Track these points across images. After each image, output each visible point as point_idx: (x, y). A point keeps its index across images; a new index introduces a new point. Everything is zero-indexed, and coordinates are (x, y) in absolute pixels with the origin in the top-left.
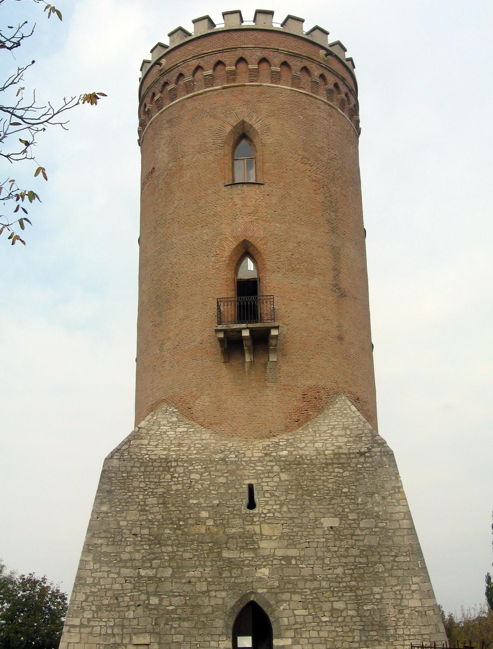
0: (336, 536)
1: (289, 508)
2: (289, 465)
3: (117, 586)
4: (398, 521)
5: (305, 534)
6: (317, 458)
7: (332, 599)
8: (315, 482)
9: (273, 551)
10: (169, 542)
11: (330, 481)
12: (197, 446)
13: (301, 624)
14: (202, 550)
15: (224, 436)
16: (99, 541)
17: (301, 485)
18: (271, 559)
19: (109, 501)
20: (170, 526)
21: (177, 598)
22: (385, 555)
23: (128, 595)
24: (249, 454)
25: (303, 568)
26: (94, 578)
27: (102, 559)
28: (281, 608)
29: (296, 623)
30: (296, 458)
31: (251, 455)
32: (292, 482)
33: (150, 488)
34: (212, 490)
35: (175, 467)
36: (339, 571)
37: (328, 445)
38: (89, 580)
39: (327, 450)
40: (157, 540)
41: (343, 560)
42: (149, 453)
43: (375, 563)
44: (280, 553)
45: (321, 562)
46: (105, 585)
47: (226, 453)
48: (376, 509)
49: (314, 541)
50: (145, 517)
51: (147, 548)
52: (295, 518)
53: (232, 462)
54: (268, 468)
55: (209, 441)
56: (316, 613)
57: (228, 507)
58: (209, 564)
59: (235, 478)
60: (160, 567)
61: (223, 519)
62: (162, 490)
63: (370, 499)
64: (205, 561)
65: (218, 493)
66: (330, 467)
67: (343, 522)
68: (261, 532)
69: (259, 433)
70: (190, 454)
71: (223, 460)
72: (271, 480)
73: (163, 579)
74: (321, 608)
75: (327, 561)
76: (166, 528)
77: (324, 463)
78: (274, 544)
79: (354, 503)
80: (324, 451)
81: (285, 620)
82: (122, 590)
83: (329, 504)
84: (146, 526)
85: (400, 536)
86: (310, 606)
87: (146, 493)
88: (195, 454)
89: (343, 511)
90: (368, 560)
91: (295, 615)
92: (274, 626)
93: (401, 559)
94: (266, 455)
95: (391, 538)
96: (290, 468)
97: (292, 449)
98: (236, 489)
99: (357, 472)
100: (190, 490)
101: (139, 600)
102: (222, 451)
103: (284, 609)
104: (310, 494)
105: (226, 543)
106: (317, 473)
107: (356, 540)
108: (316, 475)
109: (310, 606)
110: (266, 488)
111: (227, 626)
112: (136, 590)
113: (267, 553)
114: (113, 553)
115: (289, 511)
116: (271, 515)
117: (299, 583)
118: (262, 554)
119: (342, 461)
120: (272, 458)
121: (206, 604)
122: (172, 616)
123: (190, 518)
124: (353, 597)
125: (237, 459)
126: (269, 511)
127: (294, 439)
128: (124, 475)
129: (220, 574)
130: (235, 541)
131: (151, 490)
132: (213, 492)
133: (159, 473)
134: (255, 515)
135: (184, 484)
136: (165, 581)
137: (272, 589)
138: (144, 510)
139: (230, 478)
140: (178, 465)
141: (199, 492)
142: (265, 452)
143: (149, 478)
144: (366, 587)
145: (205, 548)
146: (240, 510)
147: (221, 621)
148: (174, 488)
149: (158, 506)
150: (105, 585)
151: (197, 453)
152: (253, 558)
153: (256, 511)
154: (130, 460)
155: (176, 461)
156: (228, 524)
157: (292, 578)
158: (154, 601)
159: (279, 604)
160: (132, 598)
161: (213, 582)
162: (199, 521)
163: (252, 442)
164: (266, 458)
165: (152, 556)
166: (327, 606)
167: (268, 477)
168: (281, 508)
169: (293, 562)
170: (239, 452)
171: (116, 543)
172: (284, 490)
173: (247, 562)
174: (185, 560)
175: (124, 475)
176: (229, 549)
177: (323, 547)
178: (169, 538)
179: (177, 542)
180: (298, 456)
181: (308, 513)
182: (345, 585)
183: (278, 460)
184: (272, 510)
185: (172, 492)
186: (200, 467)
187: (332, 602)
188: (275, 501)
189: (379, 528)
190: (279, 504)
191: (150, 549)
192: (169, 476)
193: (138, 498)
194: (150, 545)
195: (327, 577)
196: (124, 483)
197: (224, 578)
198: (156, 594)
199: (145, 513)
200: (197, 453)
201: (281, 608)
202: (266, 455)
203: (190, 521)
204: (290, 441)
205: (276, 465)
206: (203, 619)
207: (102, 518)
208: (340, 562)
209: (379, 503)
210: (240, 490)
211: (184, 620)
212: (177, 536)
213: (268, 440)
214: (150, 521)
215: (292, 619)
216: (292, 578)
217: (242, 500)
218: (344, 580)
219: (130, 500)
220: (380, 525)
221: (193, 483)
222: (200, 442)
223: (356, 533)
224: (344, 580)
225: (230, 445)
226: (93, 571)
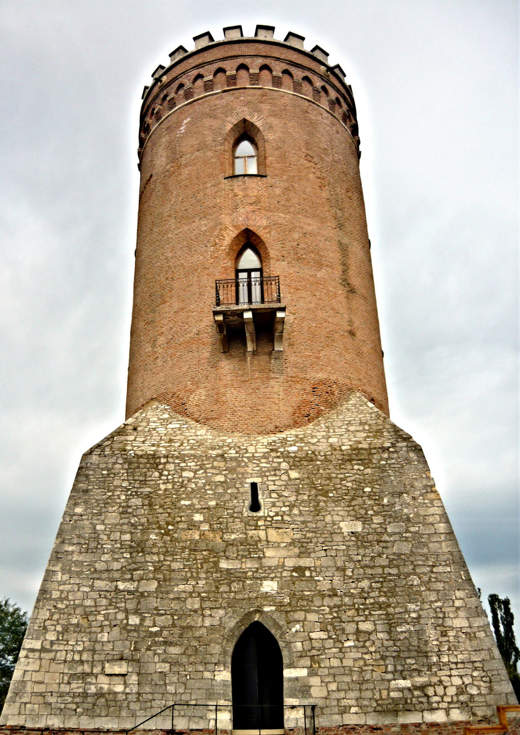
0: (359, 543)
1: (300, 511)
2: (300, 461)
3: (89, 603)
4: (433, 524)
5: (321, 540)
6: (332, 454)
7: (356, 619)
8: (331, 481)
9: (282, 560)
10: (155, 550)
11: (349, 479)
12: (191, 442)
13: (319, 650)
14: (195, 559)
15: (222, 432)
16: (71, 548)
17: (315, 485)
18: (280, 570)
19: (84, 502)
20: (157, 531)
21: (163, 618)
22: (419, 565)
23: (102, 612)
24: (251, 449)
25: (319, 581)
26: (62, 592)
27: (73, 569)
28: (294, 630)
29: (313, 648)
30: (308, 454)
31: (254, 451)
32: (303, 480)
33: (134, 487)
34: (208, 490)
35: (165, 464)
36: (365, 584)
37: (344, 441)
38: (56, 595)
39: (343, 445)
40: (139, 547)
41: (369, 571)
42: (135, 448)
43: (409, 575)
44: (290, 563)
45: (342, 573)
46: (74, 601)
47: (225, 449)
48: (405, 511)
49: (332, 549)
50: (126, 521)
51: (128, 556)
52: (308, 522)
53: (231, 459)
54: (274, 465)
55: (205, 437)
56: (337, 636)
57: (227, 509)
58: (203, 575)
59: (235, 476)
60: (142, 579)
61: (221, 523)
62: (148, 489)
63: (397, 500)
64: (198, 573)
65: (215, 493)
66: (348, 463)
67: (366, 526)
68: (267, 538)
69: (264, 428)
70: (183, 450)
71: (222, 456)
72: (278, 478)
73: (146, 594)
74: (343, 630)
75: (349, 573)
76: (151, 533)
77: (341, 460)
78: (283, 553)
79: (379, 505)
80: (340, 447)
81: (299, 645)
82: (96, 606)
83: (349, 506)
84: (128, 530)
85: (436, 542)
86: (329, 627)
87: (129, 492)
88: (189, 450)
89: (366, 514)
90: (399, 571)
91: (311, 639)
92: (285, 653)
93: (440, 569)
94: (272, 450)
95: (425, 545)
96: (301, 465)
97: (303, 445)
98: (237, 488)
99: (382, 468)
100: (182, 490)
101: (116, 619)
102: (220, 447)
103: (297, 631)
104: (325, 494)
105: (225, 552)
106: (333, 470)
107: (383, 547)
108: (332, 473)
109: (329, 627)
110: (271, 488)
111: (224, 653)
112: (113, 607)
113: (273, 563)
114: (85, 562)
115: (301, 514)
116: (279, 518)
117: (314, 599)
118: (269, 564)
119: (362, 457)
120: (279, 454)
121: (199, 625)
122: (156, 639)
123: (181, 521)
124: (383, 617)
125: (237, 455)
126: (277, 514)
127: (304, 434)
128: (105, 472)
129: (217, 588)
130: (235, 549)
131: (135, 490)
132: (209, 492)
133: (145, 470)
134: (259, 518)
135: (174, 483)
136: (148, 596)
137: (281, 606)
138: (126, 512)
139: (230, 476)
140: (167, 462)
141: (192, 492)
142: (271, 448)
143: (134, 476)
144: (398, 603)
145: (198, 557)
146: (241, 513)
147: (218, 647)
148: (163, 487)
149: (143, 508)
150: (74, 601)
151: (192, 449)
152: (257, 569)
153: (261, 514)
154: (112, 456)
155: (166, 457)
156: (227, 528)
157: (306, 593)
158: (134, 620)
159: (291, 625)
160: (107, 617)
161: (209, 598)
162: (193, 525)
163: (255, 438)
164: (272, 454)
165: (134, 566)
166: (350, 628)
167: (275, 475)
168: (291, 510)
169: (308, 574)
170: (240, 448)
171: (90, 551)
172: (294, 490)
173: (250, 574)
174: (174, 570)
175: (105, 472)
176: (227, 558)
177: (344, 556)
178: (154, 545)
179: (164, 550)
180: (310, 452)
181: (324, 516)
182: (372, 601)
183: (286, 456)
184: (281, 513)
185: (160, 492)
186: (194, 464)
187: (357, 623)
188: (284, 503)
189: (411, 532)
190: (288, 506)
191: (131, 557)
192: (157, 474)
193: (119, 498)
194: (131, 553)
195: (350, 592)
196: (104, 482)
197: (222, 593)
198: (137, 612)
199: (127, 516)
200: (192, 449)
201: (294, 630)
202: (272, 450)
203: (181, 526)
204: (300, 436)
205: (284, 461)
206: (195, 643)
207: (76, 521)
208: (365, 574)
209: (408, 504)
210: (241, 490)
211: (171, 644)
212: (165, 543)
213: (273, 435)
214: (132, 525)
215: (307, 643)
216: (306, 593)
217: (244, 501)
218: (371, 595)
219: (110, 501)
220: (412, 529)
221: (186, 482)
222: (195, 438)
223: (383, 539)
224: (371, 595)
225: (229, 441)
226: (60, 583)
